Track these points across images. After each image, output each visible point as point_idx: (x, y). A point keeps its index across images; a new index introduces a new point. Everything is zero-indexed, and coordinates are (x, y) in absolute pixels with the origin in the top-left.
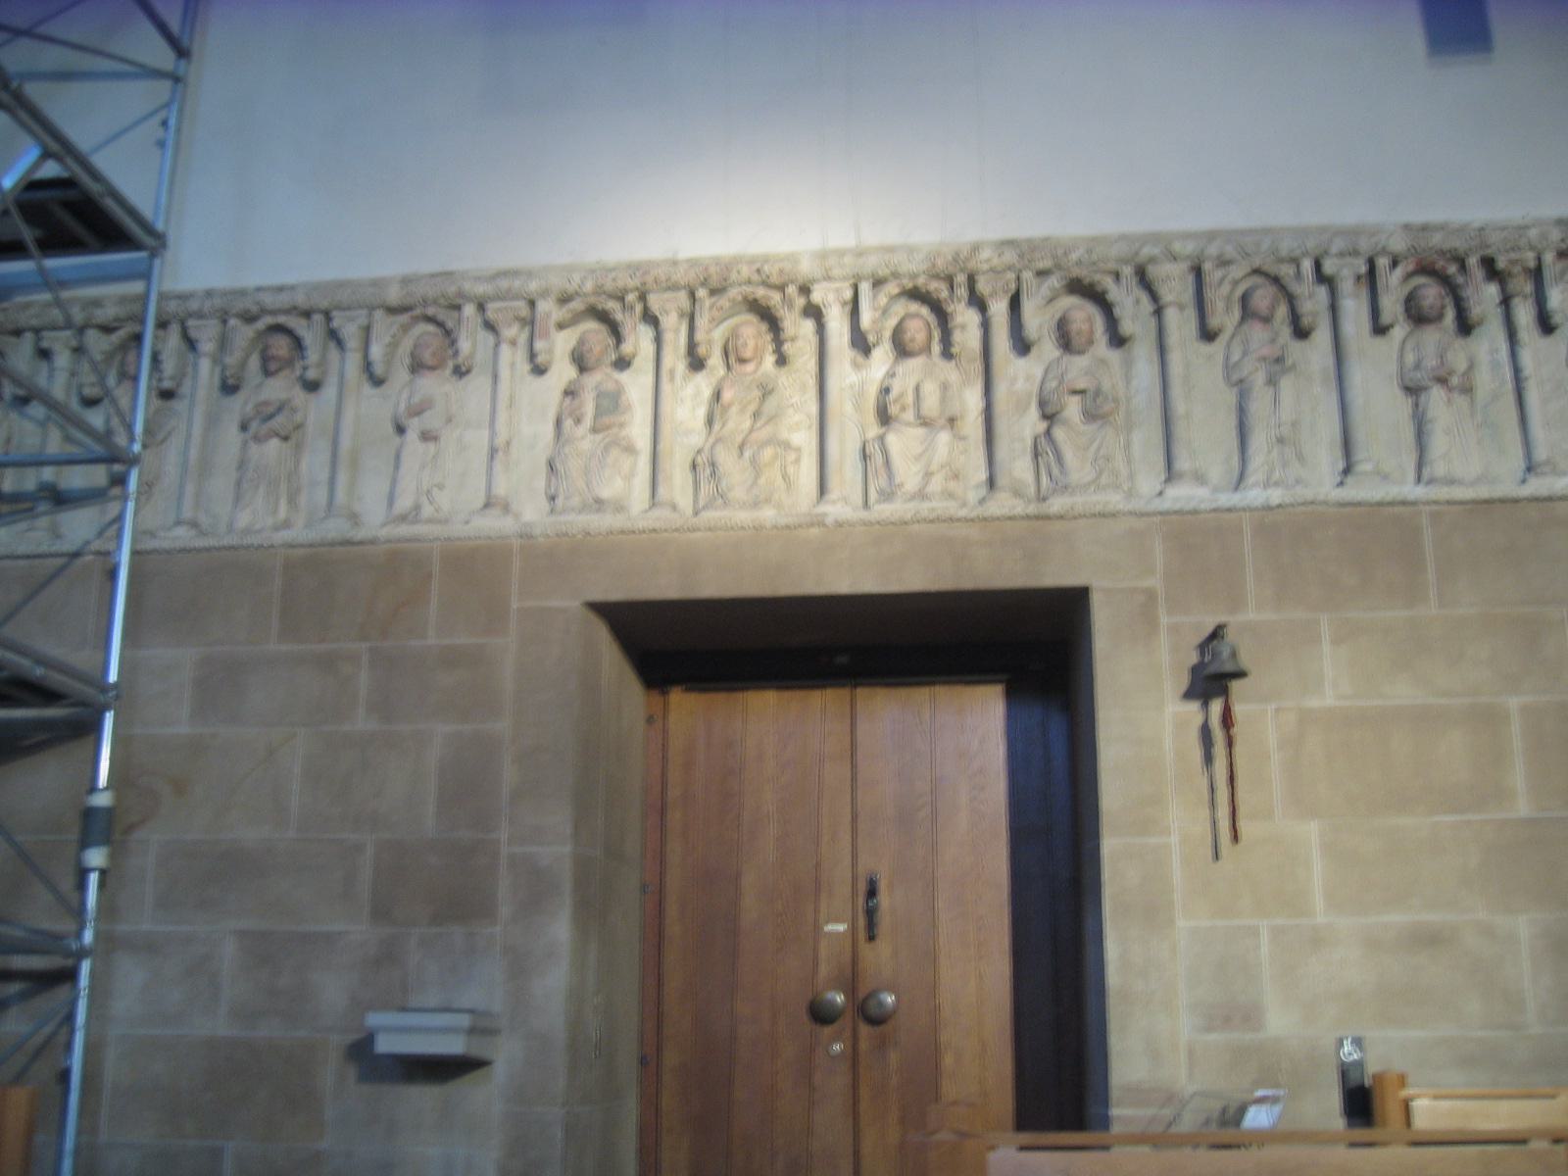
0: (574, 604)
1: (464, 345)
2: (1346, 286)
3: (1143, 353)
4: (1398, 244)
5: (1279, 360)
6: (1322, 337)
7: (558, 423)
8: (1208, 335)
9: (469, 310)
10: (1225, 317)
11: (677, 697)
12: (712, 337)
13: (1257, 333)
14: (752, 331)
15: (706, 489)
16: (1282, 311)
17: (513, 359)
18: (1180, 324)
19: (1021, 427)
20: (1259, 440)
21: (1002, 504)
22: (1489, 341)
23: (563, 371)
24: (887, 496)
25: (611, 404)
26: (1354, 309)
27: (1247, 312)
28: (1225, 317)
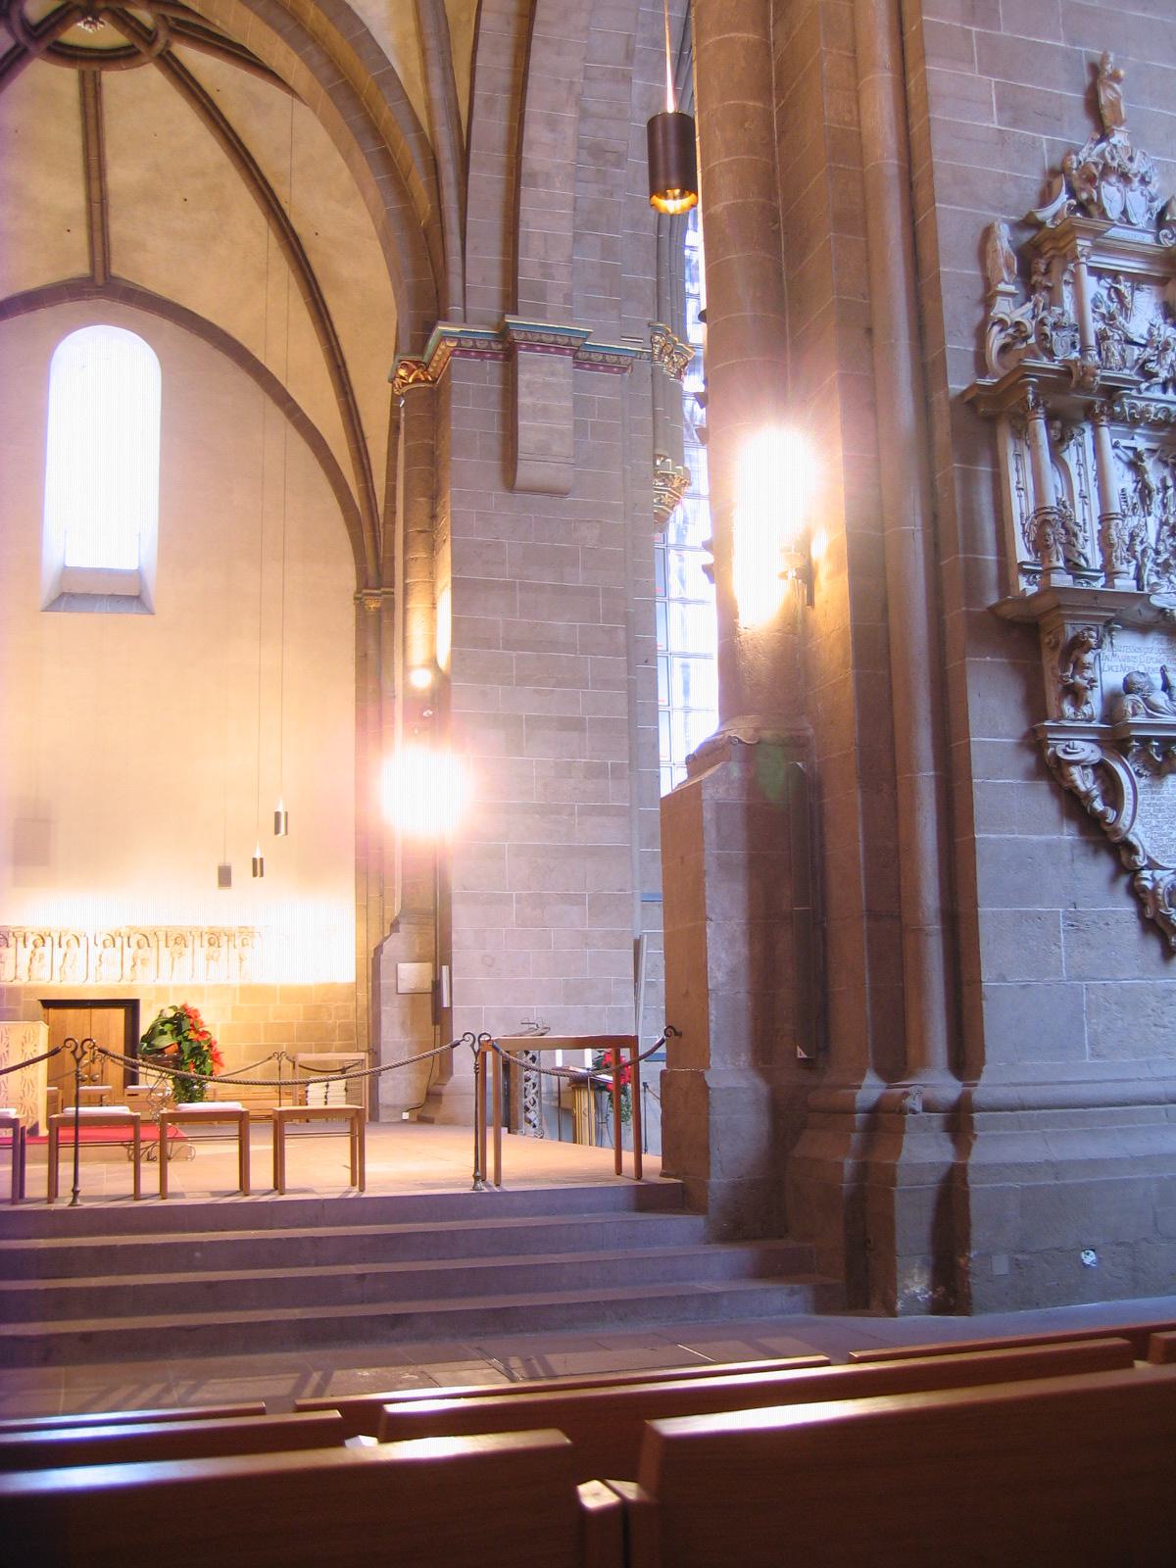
0: (36, 1000)
1: (10, 942)
2: (196, 938)
3: (155, 950)
4: (206, 930)
5: (181, 953)
6: (190, 948)
7: (31, 960)
8: (167, 946)
9: (11, 934)
10: (171, 943)
11: (51, 1010)
12: (64, 943)
13: (177, 947)
14: (74, 942)
15: (63, 976)
16: (183, 942)
17: (20, 944)
18: (162, 943)
19: (128, 964)
20: (175, 969)
21: (124, 983)
22: (224, 950)
23: (30, 946)
24: (101, 979)
25: (42, 956)
26: (198, 942)
27: (176, 943)
28: (171, 943)
